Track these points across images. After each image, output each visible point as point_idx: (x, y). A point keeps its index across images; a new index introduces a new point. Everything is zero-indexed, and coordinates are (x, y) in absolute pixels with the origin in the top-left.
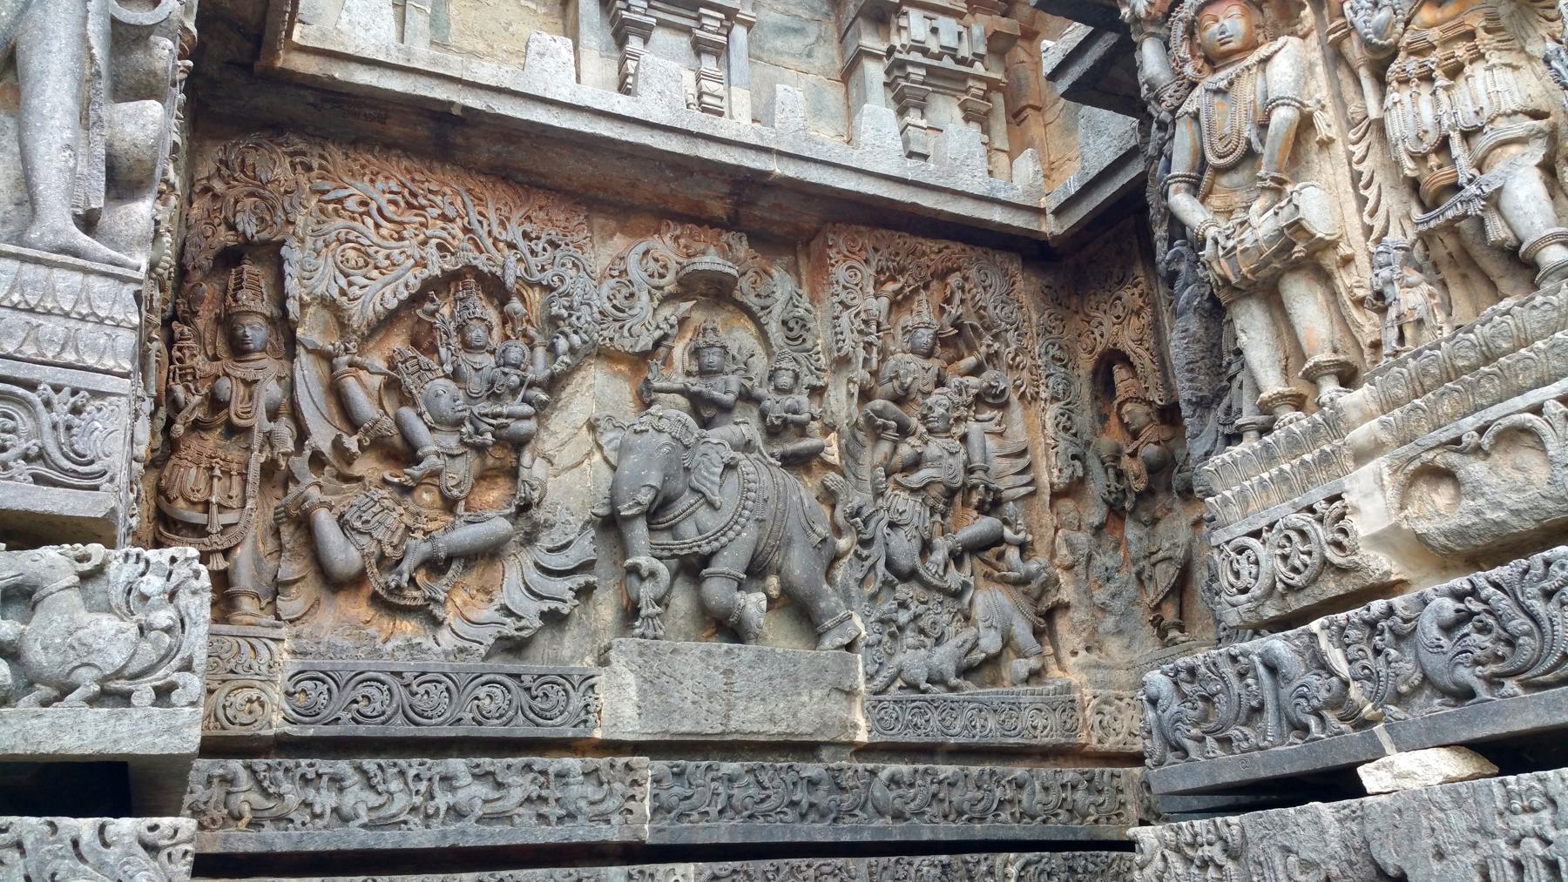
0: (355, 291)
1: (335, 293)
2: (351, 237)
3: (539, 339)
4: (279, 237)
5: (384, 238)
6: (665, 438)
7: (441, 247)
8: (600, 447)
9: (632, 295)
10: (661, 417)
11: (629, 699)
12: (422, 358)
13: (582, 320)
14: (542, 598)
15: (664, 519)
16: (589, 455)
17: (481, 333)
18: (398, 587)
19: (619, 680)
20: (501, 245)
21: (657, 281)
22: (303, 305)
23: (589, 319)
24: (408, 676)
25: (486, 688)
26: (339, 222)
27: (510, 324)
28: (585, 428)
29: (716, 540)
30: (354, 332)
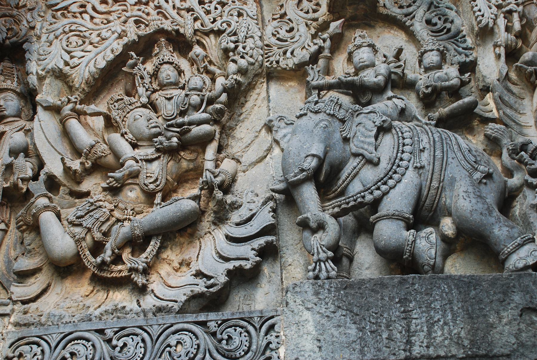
0: (76, 61)
1: (61, 65)
2: (73, 28)
3: (218, 71)
4: (24, 39)
5: (96, 24)
6: (321, 116)
7: (137, 22)
8: (277, 142)
9: (291, 30)
10: (316, 103)
11: (308, 334)
12: (126, 98)
13: (248, 48)
14: (227, 259)
15: (336, 187)
16: (269, 150)
17: (170, 73)
18: (103, 262)
19: (297, 318)
20: (183, 13)
21: (311, 15)
22: (41, 79)
23: (253, 46)
24: (109, 333)
25: (177, 336)
26: (66, 21)
27: (195, 66)
28: (264, 131)
29: (378, 189)
30: (77, 89)
